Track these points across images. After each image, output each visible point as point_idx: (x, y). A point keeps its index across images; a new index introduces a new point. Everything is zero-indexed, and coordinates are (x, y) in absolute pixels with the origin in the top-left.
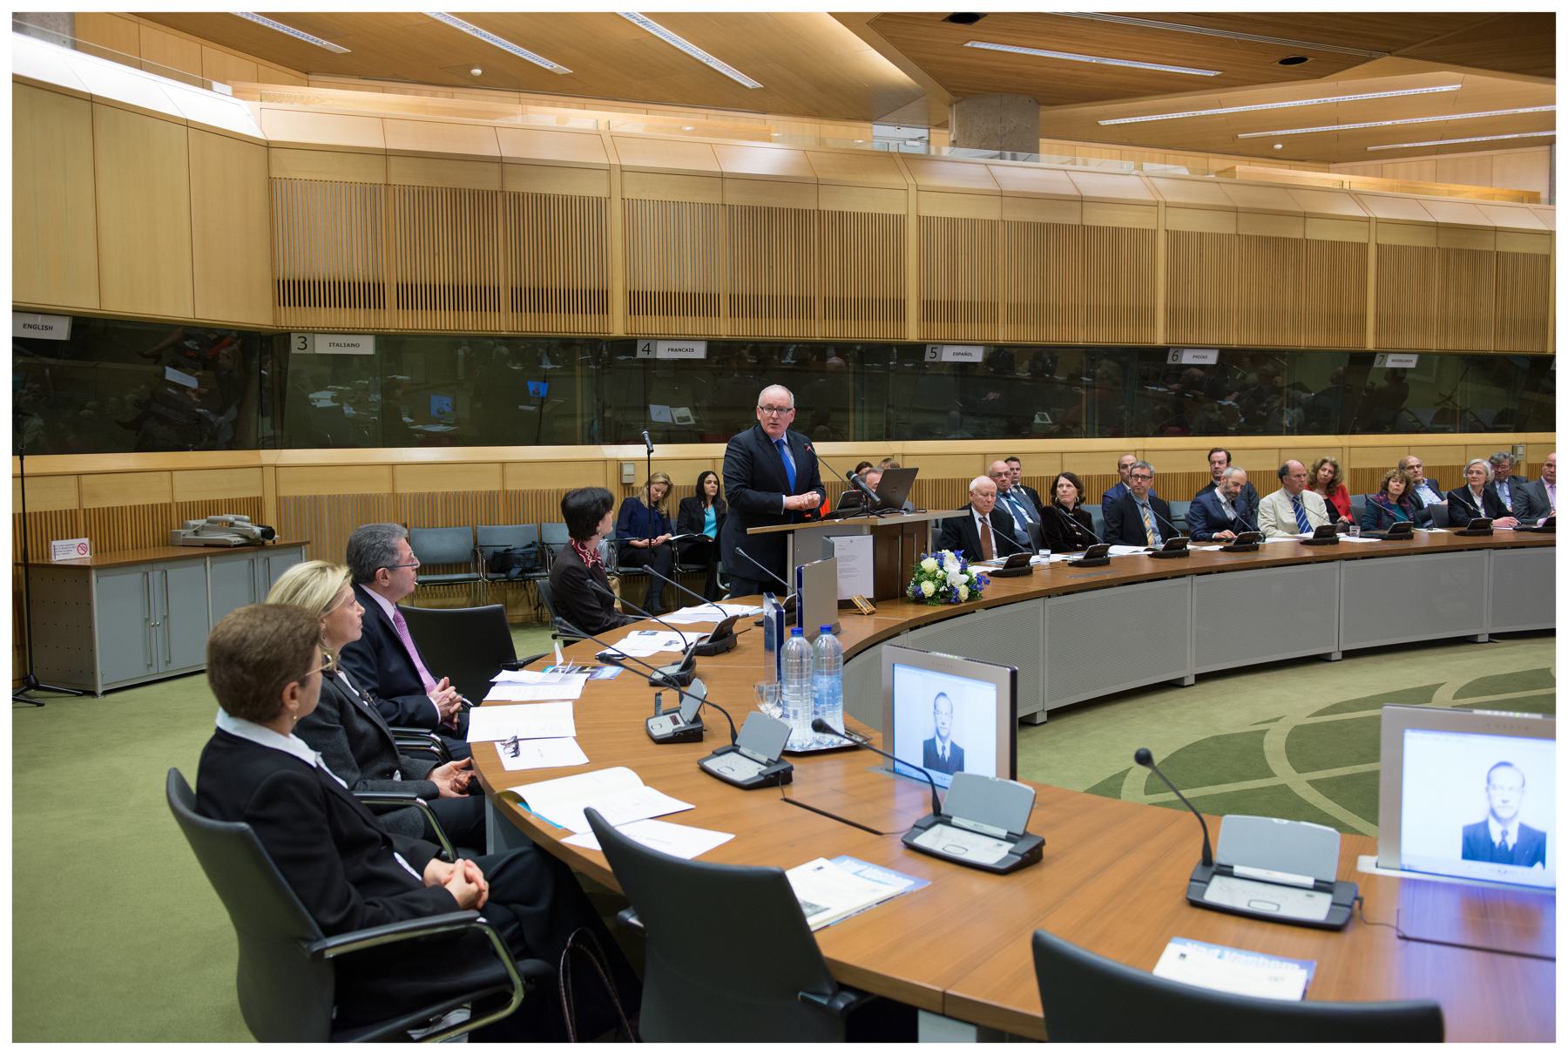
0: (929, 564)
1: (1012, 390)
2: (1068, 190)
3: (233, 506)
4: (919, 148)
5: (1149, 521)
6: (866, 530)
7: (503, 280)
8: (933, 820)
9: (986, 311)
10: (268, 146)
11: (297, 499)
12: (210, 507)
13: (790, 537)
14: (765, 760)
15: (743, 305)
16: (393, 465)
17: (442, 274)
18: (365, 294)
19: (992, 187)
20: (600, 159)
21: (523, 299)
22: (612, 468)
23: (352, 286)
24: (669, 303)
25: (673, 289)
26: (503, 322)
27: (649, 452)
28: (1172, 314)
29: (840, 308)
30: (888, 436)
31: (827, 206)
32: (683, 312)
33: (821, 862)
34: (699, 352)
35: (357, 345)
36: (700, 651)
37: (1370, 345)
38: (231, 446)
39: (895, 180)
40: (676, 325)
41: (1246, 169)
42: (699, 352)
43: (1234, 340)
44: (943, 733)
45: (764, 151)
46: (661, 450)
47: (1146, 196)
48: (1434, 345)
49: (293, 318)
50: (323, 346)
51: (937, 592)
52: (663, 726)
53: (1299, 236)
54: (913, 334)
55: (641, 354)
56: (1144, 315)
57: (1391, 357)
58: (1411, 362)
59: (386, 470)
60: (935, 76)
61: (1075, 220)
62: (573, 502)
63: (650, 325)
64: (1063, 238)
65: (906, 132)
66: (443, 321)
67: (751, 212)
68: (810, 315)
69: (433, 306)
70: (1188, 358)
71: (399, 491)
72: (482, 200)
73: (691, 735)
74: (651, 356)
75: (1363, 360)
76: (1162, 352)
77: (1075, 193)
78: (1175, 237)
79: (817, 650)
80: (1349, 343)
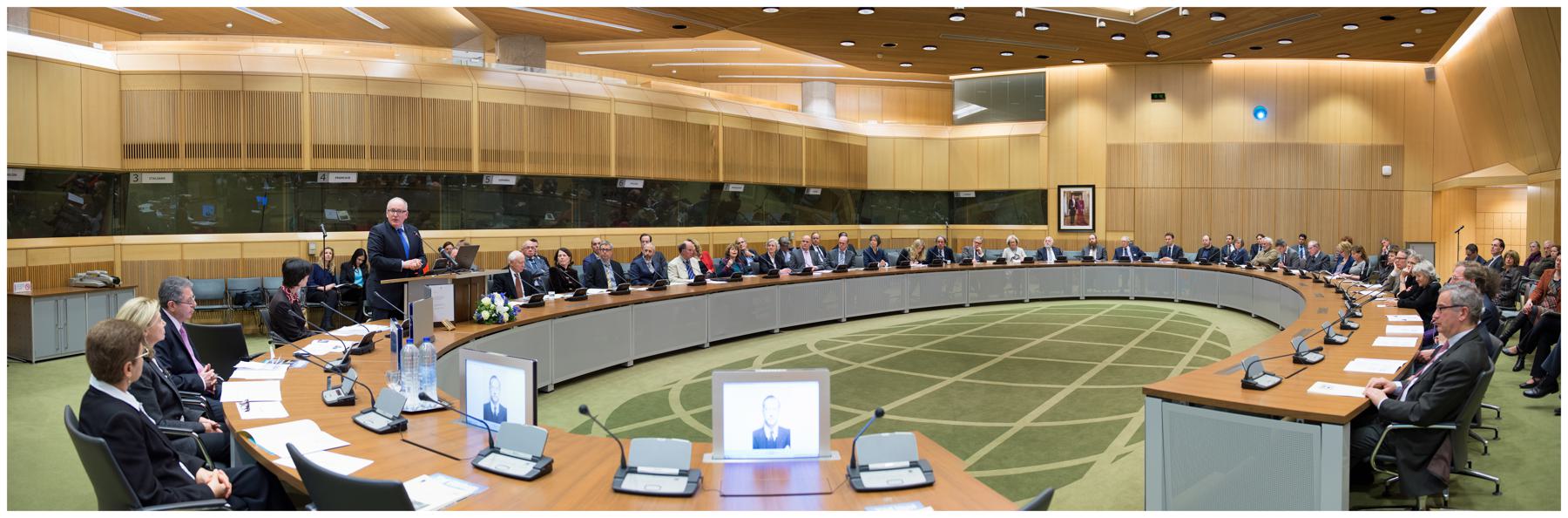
0: (486, 301)
1: (531, 201)
2: (562, 90)
3: (99, 266)
4: (478, 63)
5: (610, 274)
7: (242, 139)
9: (517, 156)
11: (132, 263)
12: (88, 266)
15: (377, 152)
17: (208, 136)
18: (169, 150)
19: (520, 86)
20: (298, 71)
21: (255, 150)
22: (303, 246)
23: (161, 146)
25: (338, 142)
26: (243, 164)
29: (433, 153)
30: (462, 227)
31: (425, 95)
33: (424, 477)
34: (353, 179)
36: (353, 352)
37: (721, 179)
38: (99, 234)
39: (465, 81)
40: (340, 163)
41: (657, 83)
42: (353, 179)
43: (652, 175)
45: (391, 64)
46: (331, 235)
48: (752, 180)
49: (132, 164)
50: (146, 179)
52: (332, 396)
54: (476, 169)
56: (604, 160)
58: (741, 189)
60: (489, 24)
63: (325, 163)
64: (559, 115)
65: (471, 54)
67: (383, 99)
68: (417, 157)
69: (204, 156)
70: (628, 184)
72: (232, 95)
73: (348, 402)
75: (717, 187)
76: (615, 180)
78: (620, 117)
80: (710, 178)
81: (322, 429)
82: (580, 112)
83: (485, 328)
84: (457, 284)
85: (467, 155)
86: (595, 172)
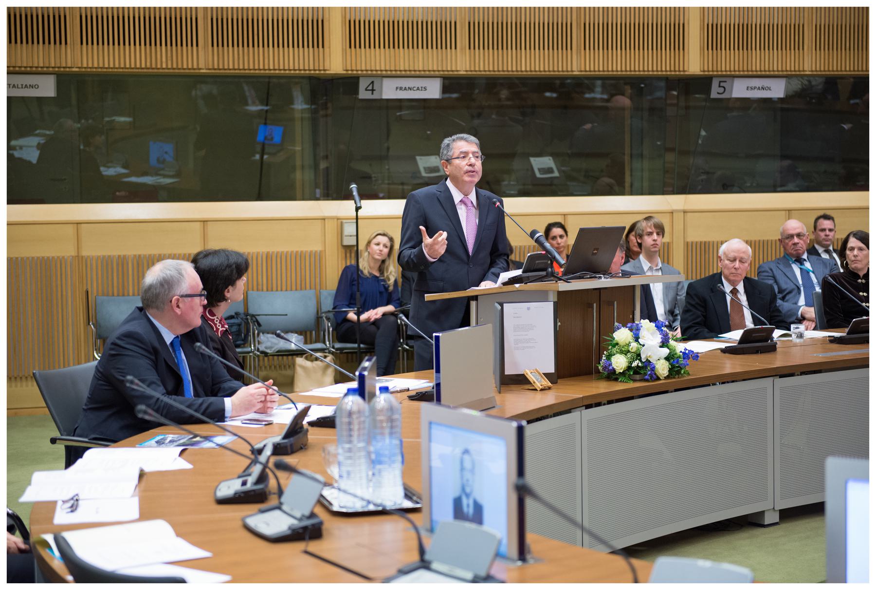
6: (553, 297)
8: (419, 564)
13: (473, 304)
14: (298, 515)
16: (78, 223)
22: (331, 227)
26: (203, 59)
27: (358, 209)
32: (412, 44)
34: (433, 90)
35: (36, 86)
42: (433, 90)
44: (468, 490)
51: (629, 368)
55: (363, 94)
59: (71, 230)
62: (205, 263)
68: (567, 45)
69: (121, 41)
71: (85, 253)
74: (376, 96)
79: (373, 411)
81: (179, 534)
83: (619, 386)
84: (565, 304)
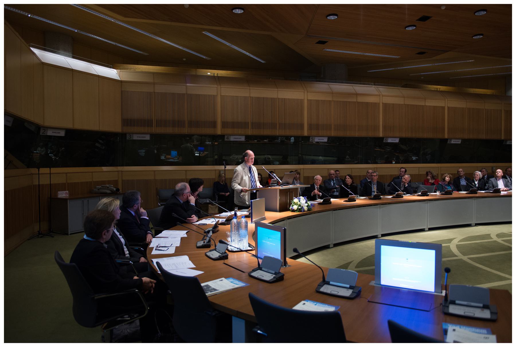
3: (109, 182)
10: (121, 82)
12: (103, 182)
18: (148, 123)
24: (234, 125)
28: (384, 127)
37: (446, 137)
43: (404, 135)
47: (377, 93)
50: (135, 137)
53: (424, 104)
54: (306, 133)
55: (226, 140)
57: (453, 140)
61: (354, 100)
63: (229, 131)
66: (169, 130)
70: (390, 141)
75: (444, 141)
76: (382, 138)
77: (355, 92)
78: (385, 105)
80: (440, 136)
82: (362, 103)
85: (302, 126)
86: (371, 134)
